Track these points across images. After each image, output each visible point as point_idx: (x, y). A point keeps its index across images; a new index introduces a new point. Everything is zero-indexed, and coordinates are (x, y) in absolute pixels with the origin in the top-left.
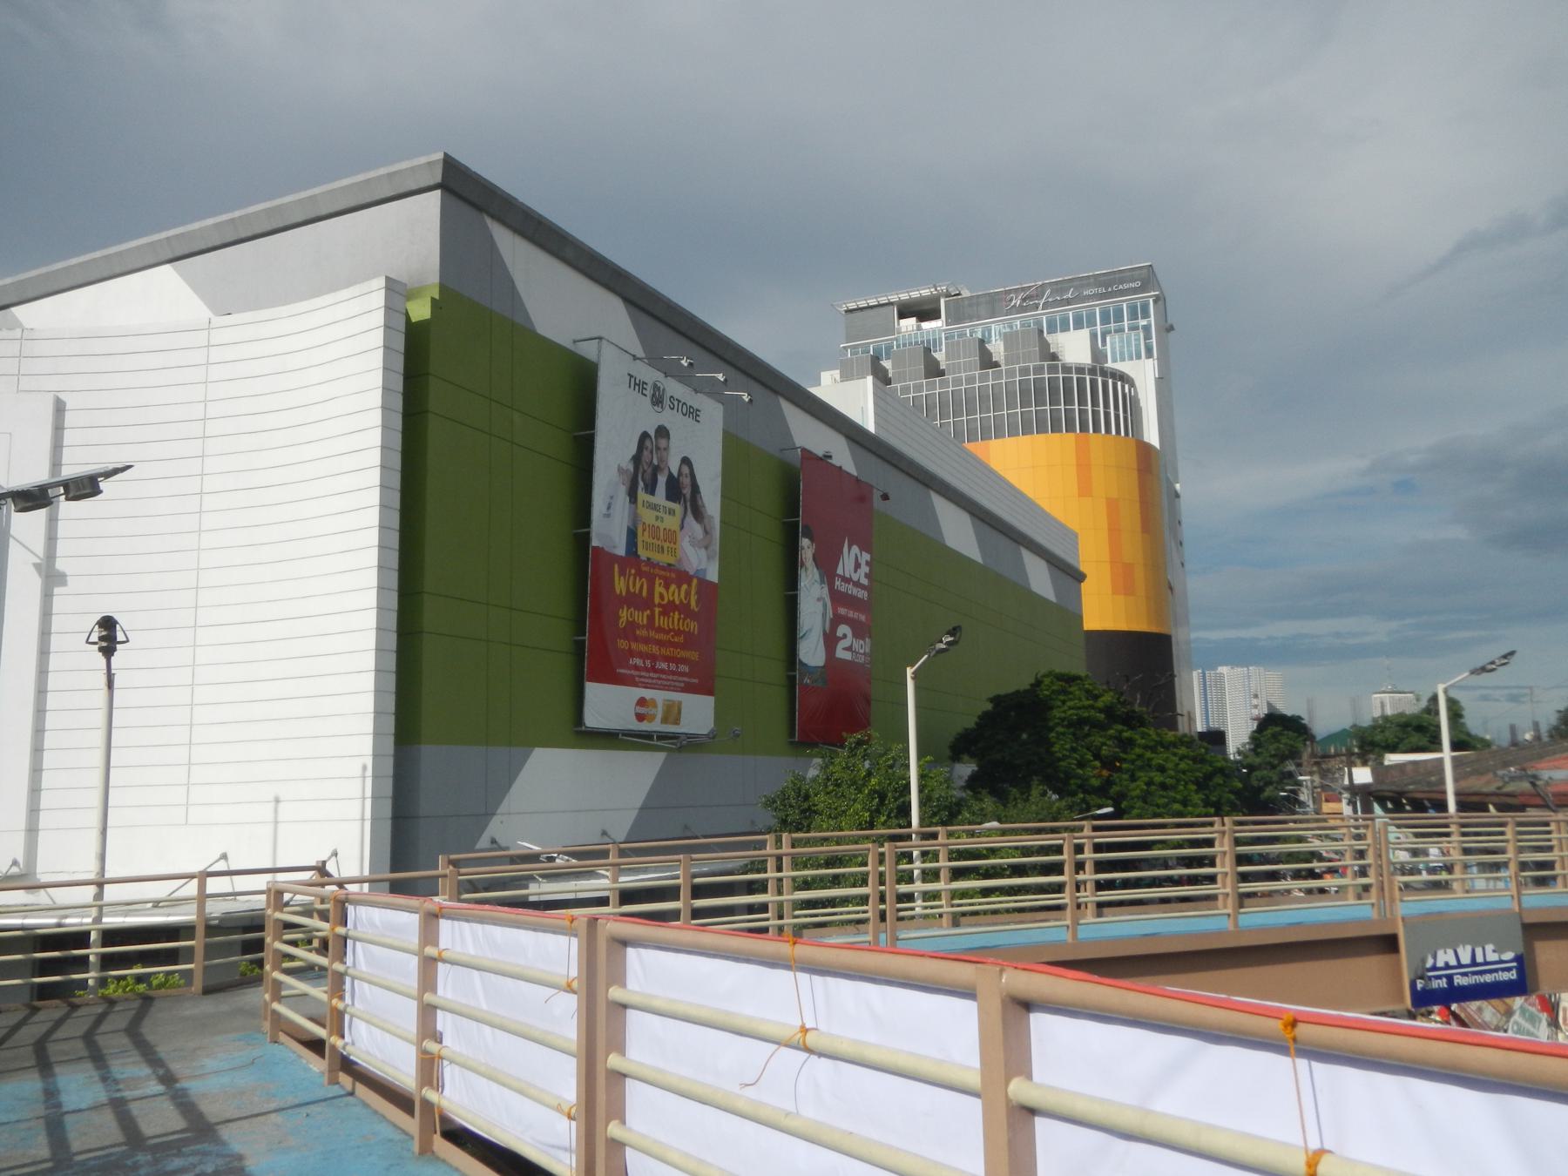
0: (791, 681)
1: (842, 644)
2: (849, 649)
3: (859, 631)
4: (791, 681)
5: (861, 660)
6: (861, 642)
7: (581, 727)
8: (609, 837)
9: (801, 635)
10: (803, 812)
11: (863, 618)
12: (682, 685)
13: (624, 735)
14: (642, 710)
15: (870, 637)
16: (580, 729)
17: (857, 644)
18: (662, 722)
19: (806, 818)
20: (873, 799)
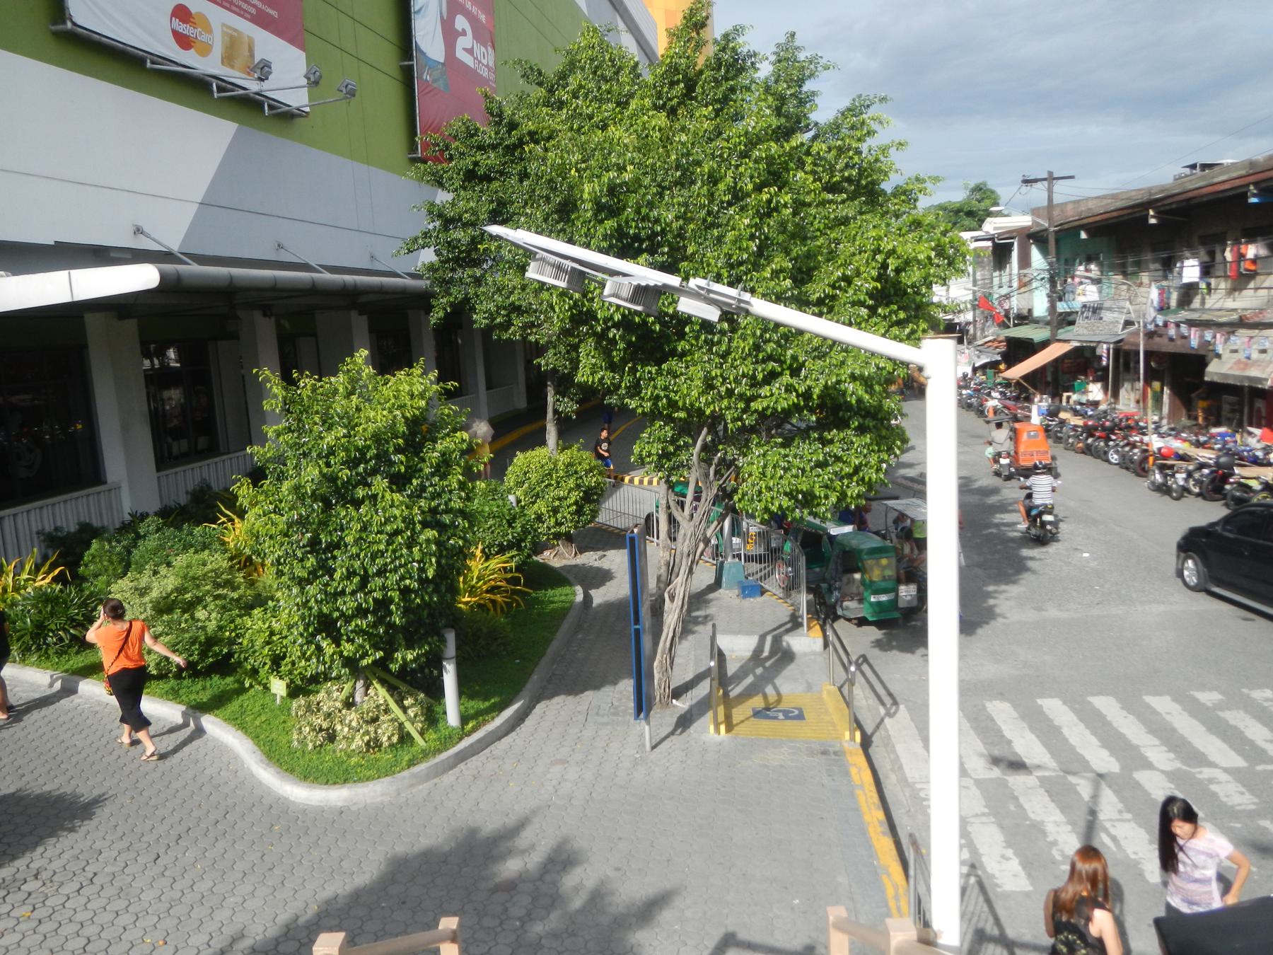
0: (407, 77)
1: (464, 42)
2: (470, 51)
3: (485, 35)
4: (407, 77)
5: (484, 73)
6: (483, 49)
7: (64, 22)
8: (148, 236)
9: (416, 9)
10: (510, 149)
11: (483, 17)
12: (253, 11)
13: (153, 62)
14: (183, 28)
15: (493, 47)
16: (60, 27)
17: (479, 50)
18: (223, 63)
19: (512, 162)
20: (673, 84)
